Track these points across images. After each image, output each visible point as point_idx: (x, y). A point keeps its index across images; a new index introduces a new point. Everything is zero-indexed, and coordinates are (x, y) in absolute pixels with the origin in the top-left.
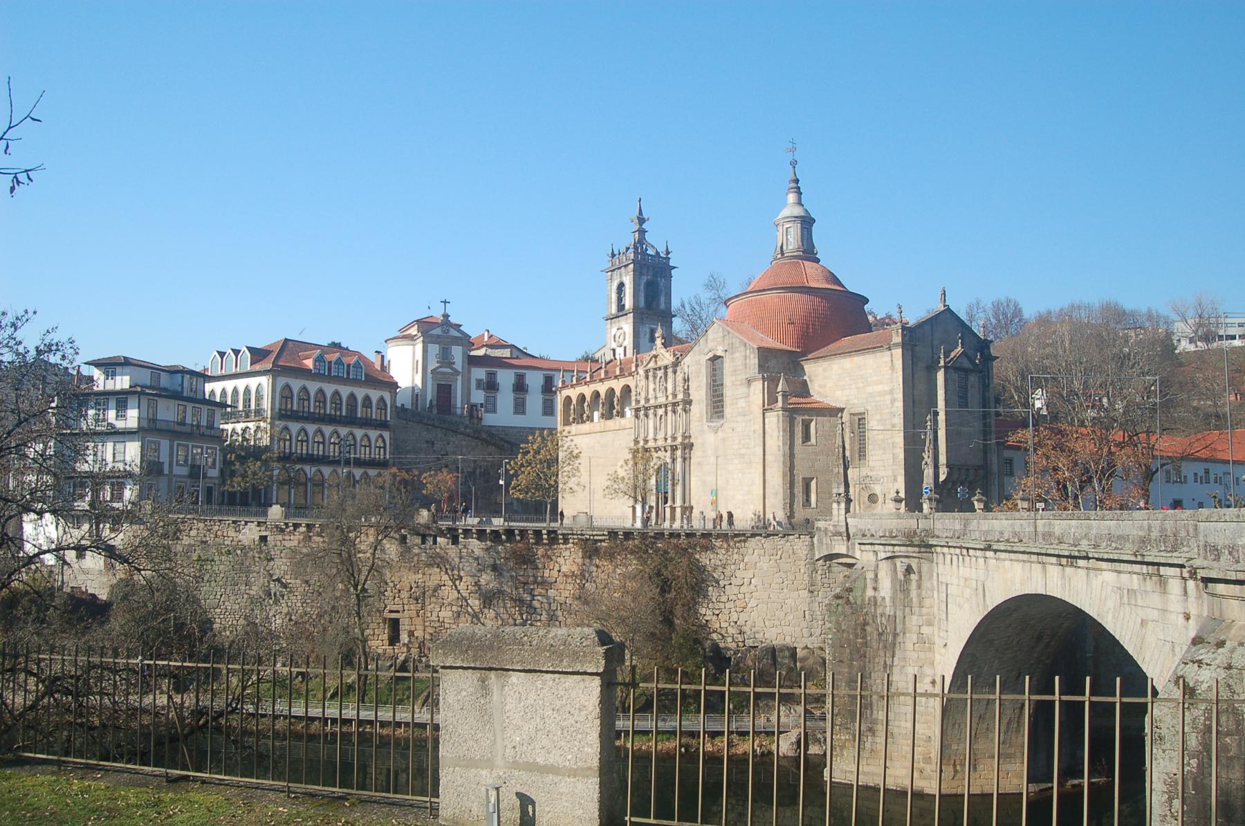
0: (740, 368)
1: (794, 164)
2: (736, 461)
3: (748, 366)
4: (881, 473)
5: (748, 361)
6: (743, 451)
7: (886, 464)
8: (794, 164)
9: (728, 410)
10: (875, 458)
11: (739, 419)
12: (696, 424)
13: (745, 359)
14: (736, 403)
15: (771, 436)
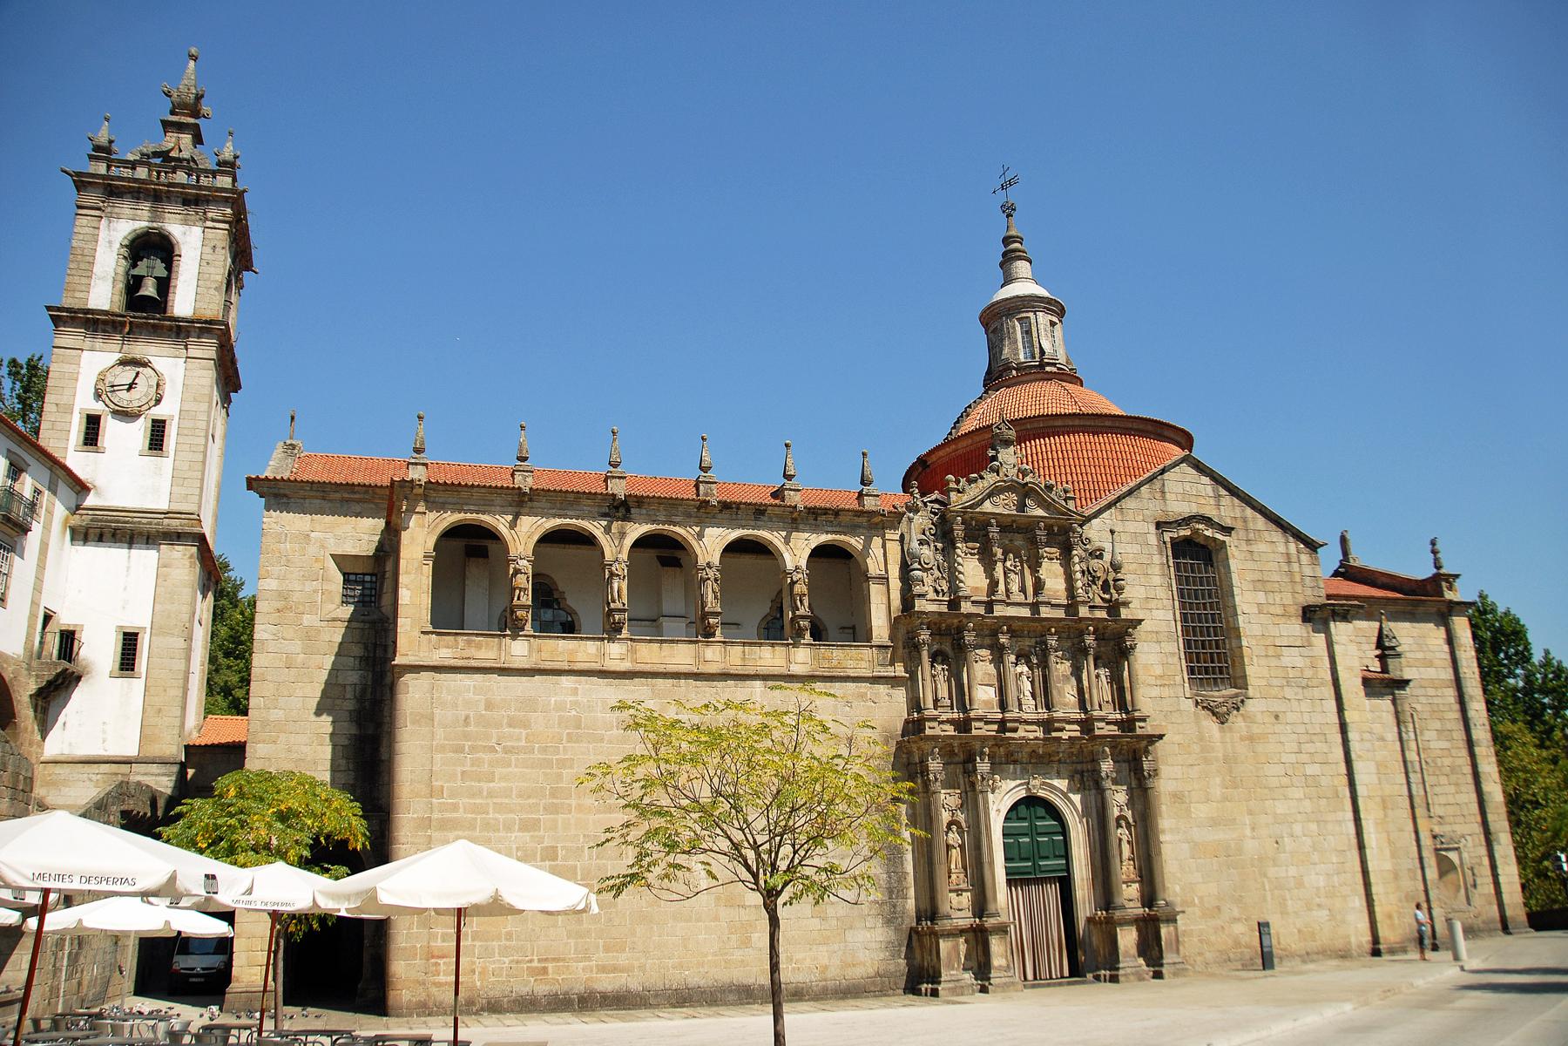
0: (1276, 577)
1: (1009, 210)
2: (1299, 793)
3: (1298, 579)
4: (1460, 829)
5: (1295, 567)
6: (1310, 770)
7: (1465, 813)
8: (1009, 210)
9: (1255, 670)
10: (1442, 800)
11: (1288, 692)
12: (1155, 692)
13: (1289, 562)
14: (1278, 656)
15: (1382, 739)
